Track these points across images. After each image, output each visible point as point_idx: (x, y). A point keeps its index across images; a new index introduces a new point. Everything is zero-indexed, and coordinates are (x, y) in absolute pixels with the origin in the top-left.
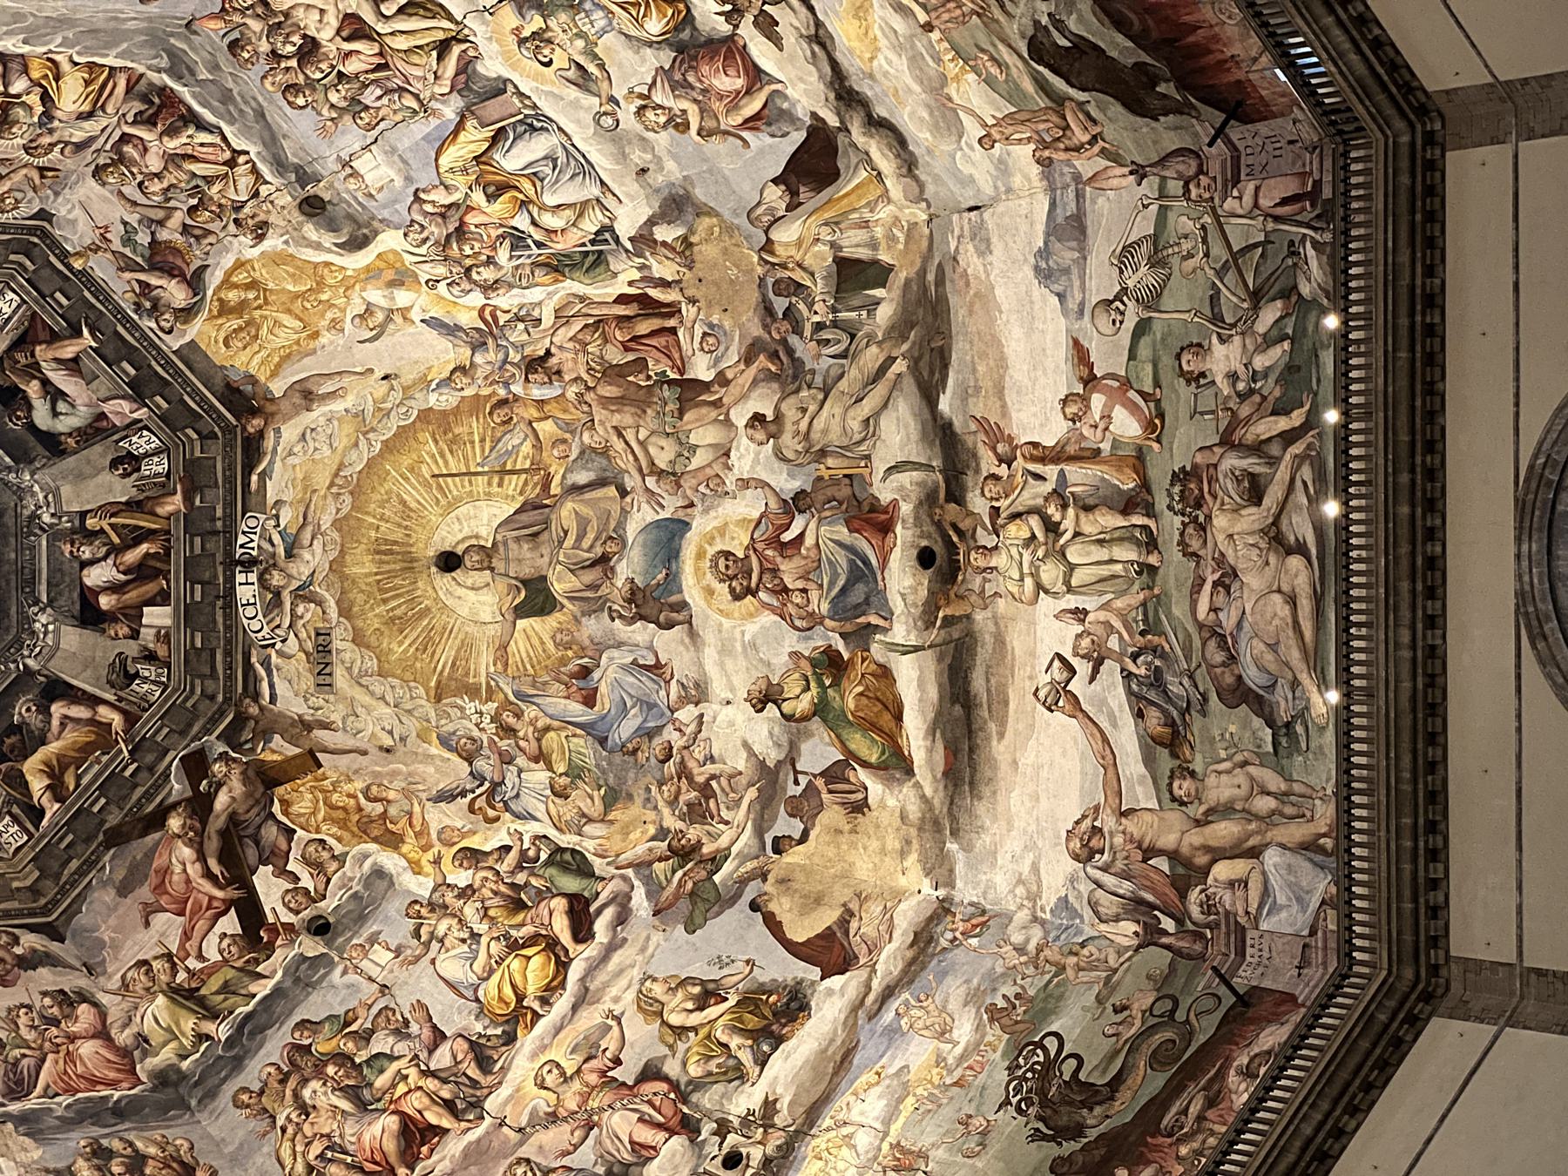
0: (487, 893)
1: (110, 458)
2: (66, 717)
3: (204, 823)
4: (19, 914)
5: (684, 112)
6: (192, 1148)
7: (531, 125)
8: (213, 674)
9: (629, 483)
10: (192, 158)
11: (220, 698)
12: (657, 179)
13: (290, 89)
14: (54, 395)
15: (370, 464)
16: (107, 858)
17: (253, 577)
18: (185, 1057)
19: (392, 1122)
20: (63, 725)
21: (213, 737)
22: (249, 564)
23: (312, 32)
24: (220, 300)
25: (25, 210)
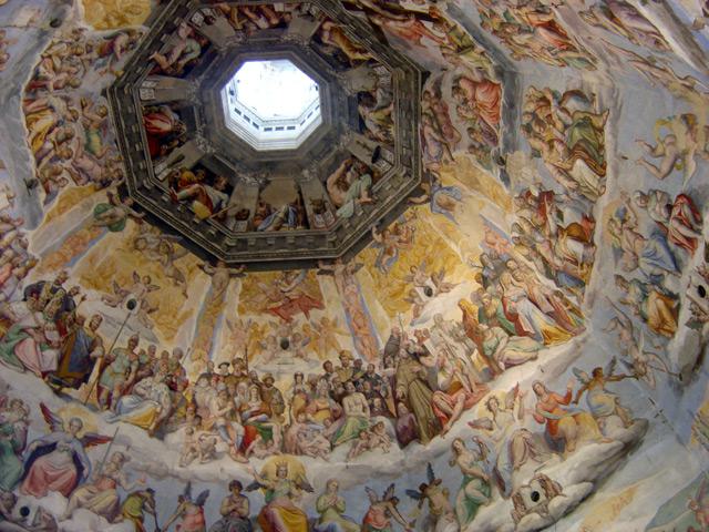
2: (329, 39)
3: (377, 13)
4: (416, 83)
10: (54, 69)
14: (183, 54)
19: (541, 31)
24: (119, 24)
25: (106, 103)
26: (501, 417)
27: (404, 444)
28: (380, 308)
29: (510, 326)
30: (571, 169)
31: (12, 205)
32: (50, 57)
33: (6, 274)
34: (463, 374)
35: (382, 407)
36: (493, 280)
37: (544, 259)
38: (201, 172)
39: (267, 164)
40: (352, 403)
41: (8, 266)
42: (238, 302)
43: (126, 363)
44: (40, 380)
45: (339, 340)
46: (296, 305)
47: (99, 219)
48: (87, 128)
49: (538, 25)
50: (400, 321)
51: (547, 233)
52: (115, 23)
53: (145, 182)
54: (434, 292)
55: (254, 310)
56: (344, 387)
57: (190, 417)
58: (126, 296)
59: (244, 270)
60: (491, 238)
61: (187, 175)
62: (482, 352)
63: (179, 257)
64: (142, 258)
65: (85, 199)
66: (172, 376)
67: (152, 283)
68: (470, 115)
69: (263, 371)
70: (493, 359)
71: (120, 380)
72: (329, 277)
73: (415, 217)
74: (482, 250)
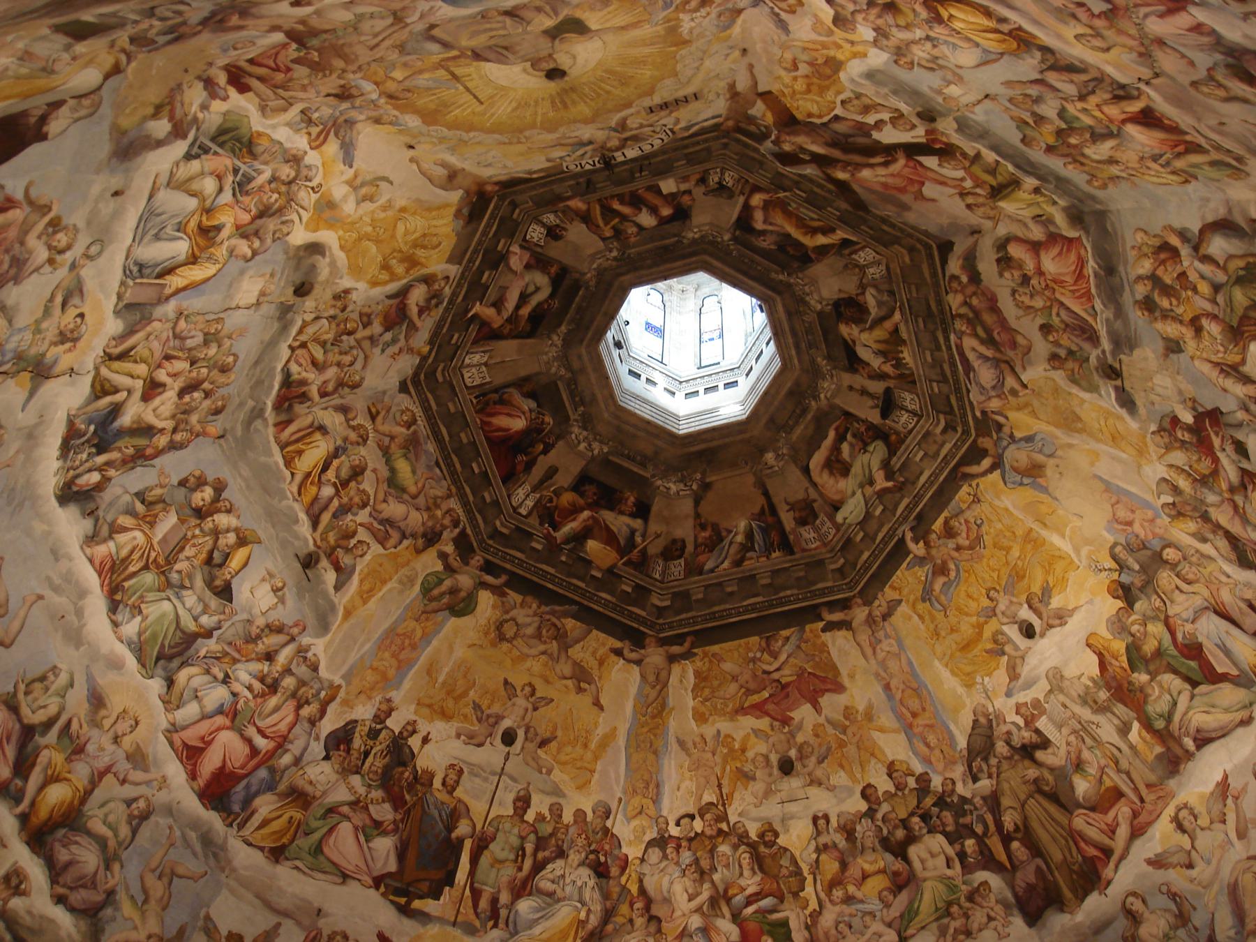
0: (880, 22)
1: (554, 244)
2: (765, 222)
4: (932, 265)
5: (39, 237)
6: (1145, 232)
7: (140, 271)
8: (708, 150)
9: (420, 27)
10: (314, 363)
11: (725, 140)
12: (116, 182)
13: (224, 370)
14: (524, 298)
15: (493, 132)
16: (878, 212)
17: (616, 154)
18: (1055, 203)
19: (1131, 129)
20: (771, 224)
21: (762, 149)
22: (608, 163)
23: (175, 399)
24: (407, 271)
25: (405, 401)
26: (1203, 840)
27: (1033, 918)
28: (945, 674)
29: (1190, 669)
30: (1243, 362)
31: (282, 600)
32: (304, 345)
33: (290, 718)
34: (1119, 771)
35: (981, 853)
36: (1142, 589)
37: (1229, 536)
38: (590, 489)
39: (700, 454)
40: (925, 855)
41: (290, 706)
42: (691, 703)
43: (515, 841)
44: (372, 892)
45: (881, 743)
46: (795, 694)
47: (430, 600)
48: (386, 451)
49: (1124, 121)
50: (986, 692)
51: (1224, 486)
52: (400, 269)
53: (498, 523)
54: (1038, 630)
55: (722, 713)
56: (905, 827)
57: (640, 922)
58: (496, 723)
59: (693, 646)
60: (1122, 514)
61: (567, 498)
62: (1147, 725)
63: (577, 641)
64: (516, 653)
65: (404, 571)
66: (595, 852)
67: (538, 694)
68: (1039, 303)
69: (755, 820)
70: (1171, 735)
71: (508, 871)
72: (843, 633)
73: (977, 500)
74: (1111, 539)
